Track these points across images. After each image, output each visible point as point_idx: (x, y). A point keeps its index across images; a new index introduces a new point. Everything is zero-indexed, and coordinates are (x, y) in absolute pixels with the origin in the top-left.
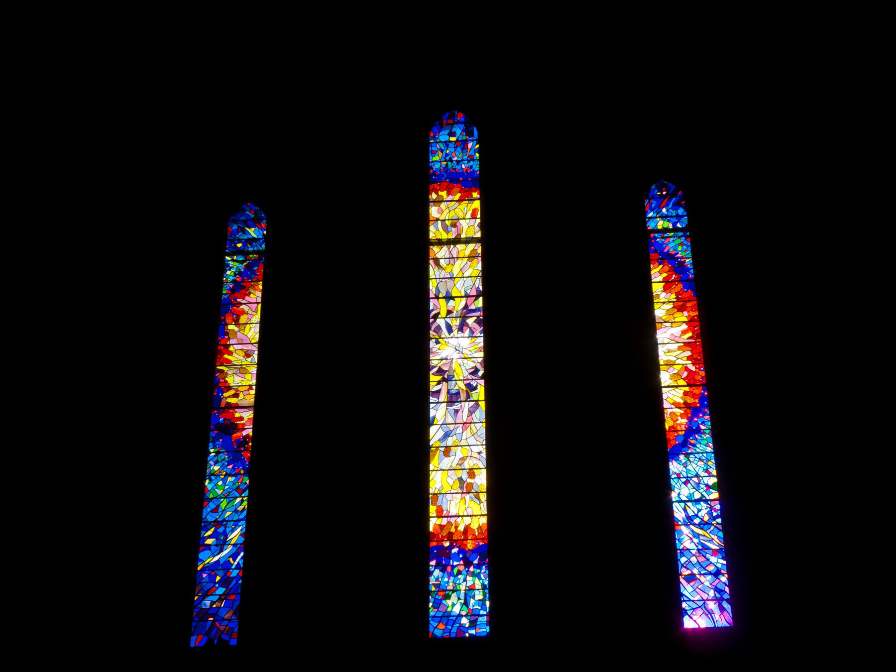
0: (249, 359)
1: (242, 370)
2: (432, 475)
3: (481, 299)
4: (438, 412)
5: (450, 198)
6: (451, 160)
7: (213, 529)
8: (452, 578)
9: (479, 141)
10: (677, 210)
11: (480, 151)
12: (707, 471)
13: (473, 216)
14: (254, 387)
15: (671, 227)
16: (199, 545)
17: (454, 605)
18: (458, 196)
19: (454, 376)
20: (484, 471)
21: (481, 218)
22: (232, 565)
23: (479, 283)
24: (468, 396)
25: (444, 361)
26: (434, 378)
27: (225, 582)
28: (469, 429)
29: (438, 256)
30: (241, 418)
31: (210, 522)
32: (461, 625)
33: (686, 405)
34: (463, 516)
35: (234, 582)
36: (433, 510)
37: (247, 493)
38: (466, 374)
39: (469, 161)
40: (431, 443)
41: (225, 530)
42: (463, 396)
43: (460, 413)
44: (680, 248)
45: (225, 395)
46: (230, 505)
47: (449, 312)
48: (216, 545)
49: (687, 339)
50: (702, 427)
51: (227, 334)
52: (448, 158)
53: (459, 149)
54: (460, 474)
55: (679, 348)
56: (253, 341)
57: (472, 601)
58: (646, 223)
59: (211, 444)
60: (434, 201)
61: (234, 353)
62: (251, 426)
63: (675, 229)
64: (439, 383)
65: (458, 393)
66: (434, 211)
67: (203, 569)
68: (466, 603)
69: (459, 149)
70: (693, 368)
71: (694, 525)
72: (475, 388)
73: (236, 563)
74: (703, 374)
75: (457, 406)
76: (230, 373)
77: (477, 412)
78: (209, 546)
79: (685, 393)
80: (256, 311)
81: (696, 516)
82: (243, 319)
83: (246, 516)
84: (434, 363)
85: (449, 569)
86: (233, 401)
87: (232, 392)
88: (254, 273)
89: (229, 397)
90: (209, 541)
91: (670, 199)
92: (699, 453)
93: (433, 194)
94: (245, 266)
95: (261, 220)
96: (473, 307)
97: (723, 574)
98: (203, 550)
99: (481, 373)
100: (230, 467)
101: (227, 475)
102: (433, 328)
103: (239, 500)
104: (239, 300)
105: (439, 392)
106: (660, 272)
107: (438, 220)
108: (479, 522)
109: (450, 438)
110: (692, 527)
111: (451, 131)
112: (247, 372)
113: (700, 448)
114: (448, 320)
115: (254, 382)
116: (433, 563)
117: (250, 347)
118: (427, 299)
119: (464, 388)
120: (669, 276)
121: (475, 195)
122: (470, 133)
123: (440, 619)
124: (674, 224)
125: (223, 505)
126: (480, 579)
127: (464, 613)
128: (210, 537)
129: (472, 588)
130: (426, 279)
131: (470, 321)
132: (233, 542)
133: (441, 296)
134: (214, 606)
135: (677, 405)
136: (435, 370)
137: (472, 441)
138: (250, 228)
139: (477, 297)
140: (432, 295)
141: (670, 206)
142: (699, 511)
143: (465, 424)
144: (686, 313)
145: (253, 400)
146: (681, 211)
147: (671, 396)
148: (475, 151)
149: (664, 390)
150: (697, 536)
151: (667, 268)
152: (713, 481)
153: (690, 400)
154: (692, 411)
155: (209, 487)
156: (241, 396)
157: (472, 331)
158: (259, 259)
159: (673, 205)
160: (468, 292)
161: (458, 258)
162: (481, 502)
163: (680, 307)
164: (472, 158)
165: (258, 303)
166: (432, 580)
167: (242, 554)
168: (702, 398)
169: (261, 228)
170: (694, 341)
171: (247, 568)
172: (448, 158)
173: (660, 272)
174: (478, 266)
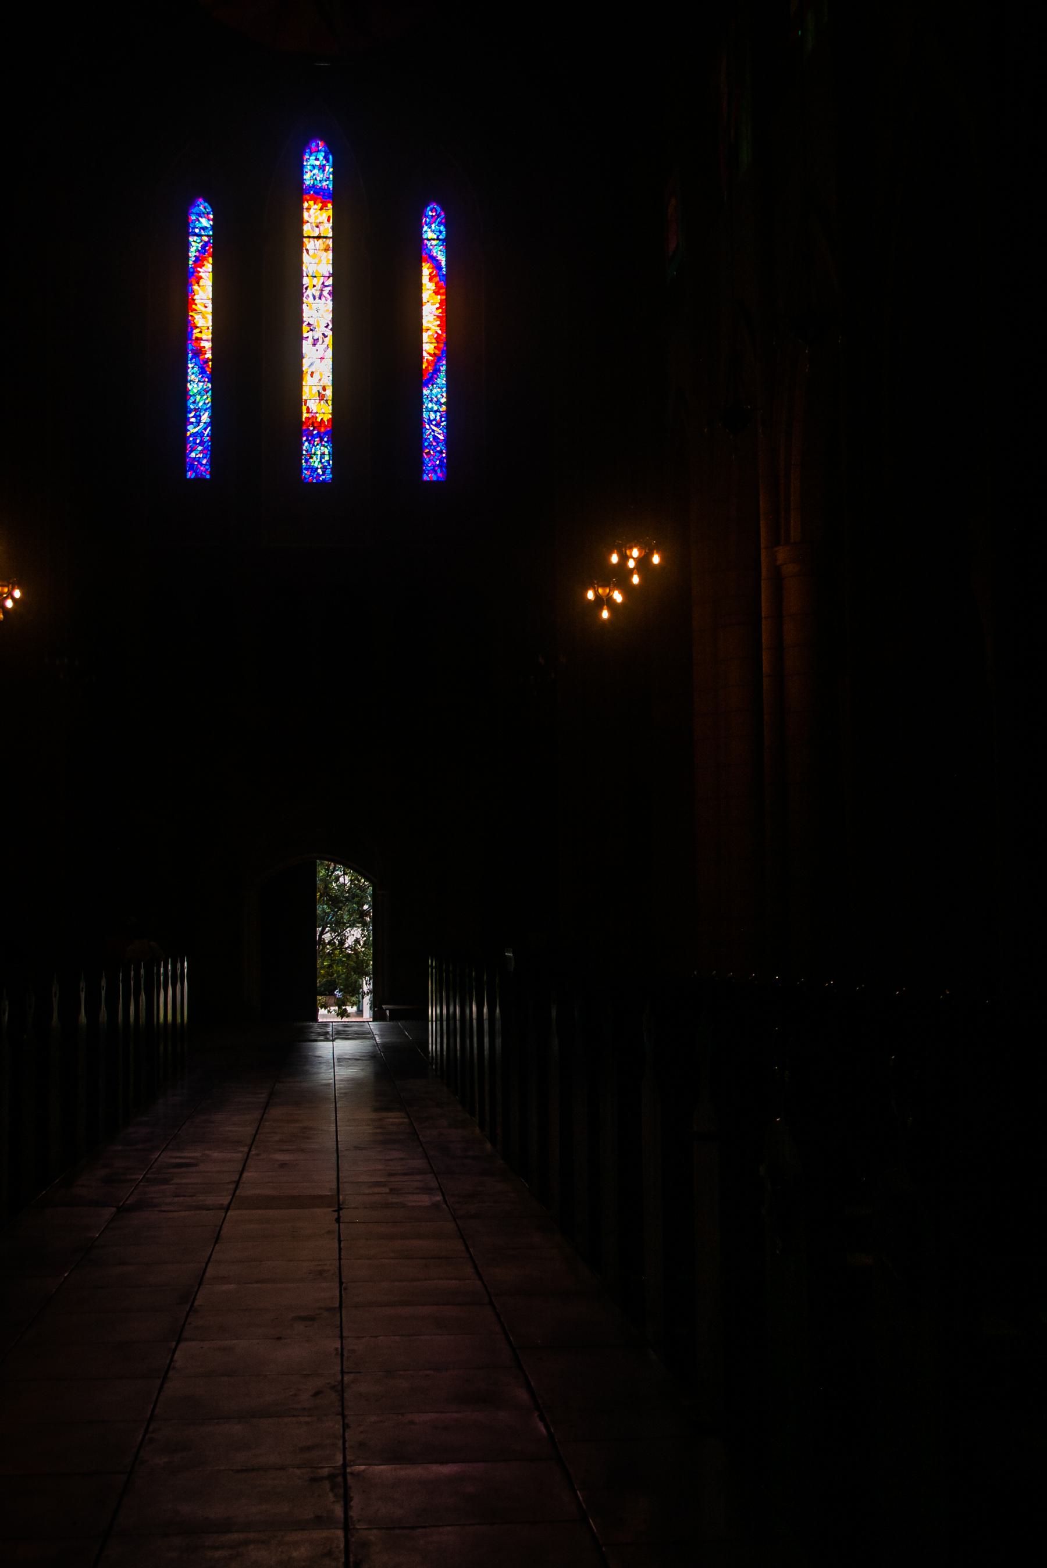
1: (204, 317)
3: (331, 278)
4: (307, 346)
5: (316, 207)
6: (316, 179)
8: (314, 447)
9: (334, 167)
10: (440, 226)
11: (333, 173)
12: (442, 395)
13: (328, 220)
14: (211, 328)
15: (435, 237)
16: (186, 422)
17: (315, 462)
18: (320, 205)
20: (331, 388)
21: (333, 223)
22: (204, 434)
23: (330, 269)
24: (323, 341)
26: (305, 328)
27: (202, 443)
29: (308, 247)
30: (204, 347)
31: (192, 409)
32: (318, 474)
33: (433, 355)
35: (207, 443)
36: (304, 408)
37: (210, 393)
39: (326, 181)
42: (321, 341)
44: (439, 253)
45: (195, 331)
48: (196, 422)
49: (440, 313)
50: (442, 369)
51: (193, 292)
53: (321, 171)
57: (323, 460)
58: (422, 234)
59: (189, 362)
60: (307, 209)
61: (198, 305)
62: (211, 352)
63: (438, 239)
65: (318, 339)
66: (306, 215)
67: (190, 436)
68: (321, 461)
69: (321, 171)
70: (440, 332)
71: (433, 425)
72: (327, 336)
74: (444, 335)
78: (192, 423)
79: (435, 347)
81: (435, 420)
82: (202, 282)
83: (210, 406)
84: (304, 319)
85: (312, 442)
86: (199, 335)
87: (198, 330)
88: (206, 251)
91: (437, 219)
92: (438, 384)
93: (306, 202)
94: (202, 246)
95: (208, 213)
96: (326, 284)
97: (444, 453)
98: (189, 425)
99: (330, 326)
101: (199, 381)
102: (305, 295)
103: (205, 397)
104: (199, 269)
105: (308, 337)
107: (308, 222)
110: (432, 426)
111: (316, 156)
113: (439, 381)
116: (304, 439)
119: (322, 336)
120: (433, 272)
121: (330, 206)
122: (327, 161)
123: (307, 469)
124: (438, 236)
125: (197, 400)
127: (319, 467)
128: (192, 417)
129: (323, 454)
131: (325, 293)
132: (204, 421)
134: (197, 456)
135: (429, 353)
139: (329, 277)
140: (305, 274)
141: (437, 223)
142: (436, 417)
144: (439, 297)
146: (442, 228)
149: (424, 345)
150: (433, 431)
151: (431, 266)
152: (443, 400)
153: (437, 352)
154: (437, 358)
155: (189, 386)
158: (209, 241)
159: (438, 224)
163: (436, 293)
164: (328, 178)
165: (209, 272)
166: (304, 448)
167: (209, 428)
169: (209, 219)
170: (441, 315)
171: (212, 436)
172: (314, 177)
174: (330, 255)
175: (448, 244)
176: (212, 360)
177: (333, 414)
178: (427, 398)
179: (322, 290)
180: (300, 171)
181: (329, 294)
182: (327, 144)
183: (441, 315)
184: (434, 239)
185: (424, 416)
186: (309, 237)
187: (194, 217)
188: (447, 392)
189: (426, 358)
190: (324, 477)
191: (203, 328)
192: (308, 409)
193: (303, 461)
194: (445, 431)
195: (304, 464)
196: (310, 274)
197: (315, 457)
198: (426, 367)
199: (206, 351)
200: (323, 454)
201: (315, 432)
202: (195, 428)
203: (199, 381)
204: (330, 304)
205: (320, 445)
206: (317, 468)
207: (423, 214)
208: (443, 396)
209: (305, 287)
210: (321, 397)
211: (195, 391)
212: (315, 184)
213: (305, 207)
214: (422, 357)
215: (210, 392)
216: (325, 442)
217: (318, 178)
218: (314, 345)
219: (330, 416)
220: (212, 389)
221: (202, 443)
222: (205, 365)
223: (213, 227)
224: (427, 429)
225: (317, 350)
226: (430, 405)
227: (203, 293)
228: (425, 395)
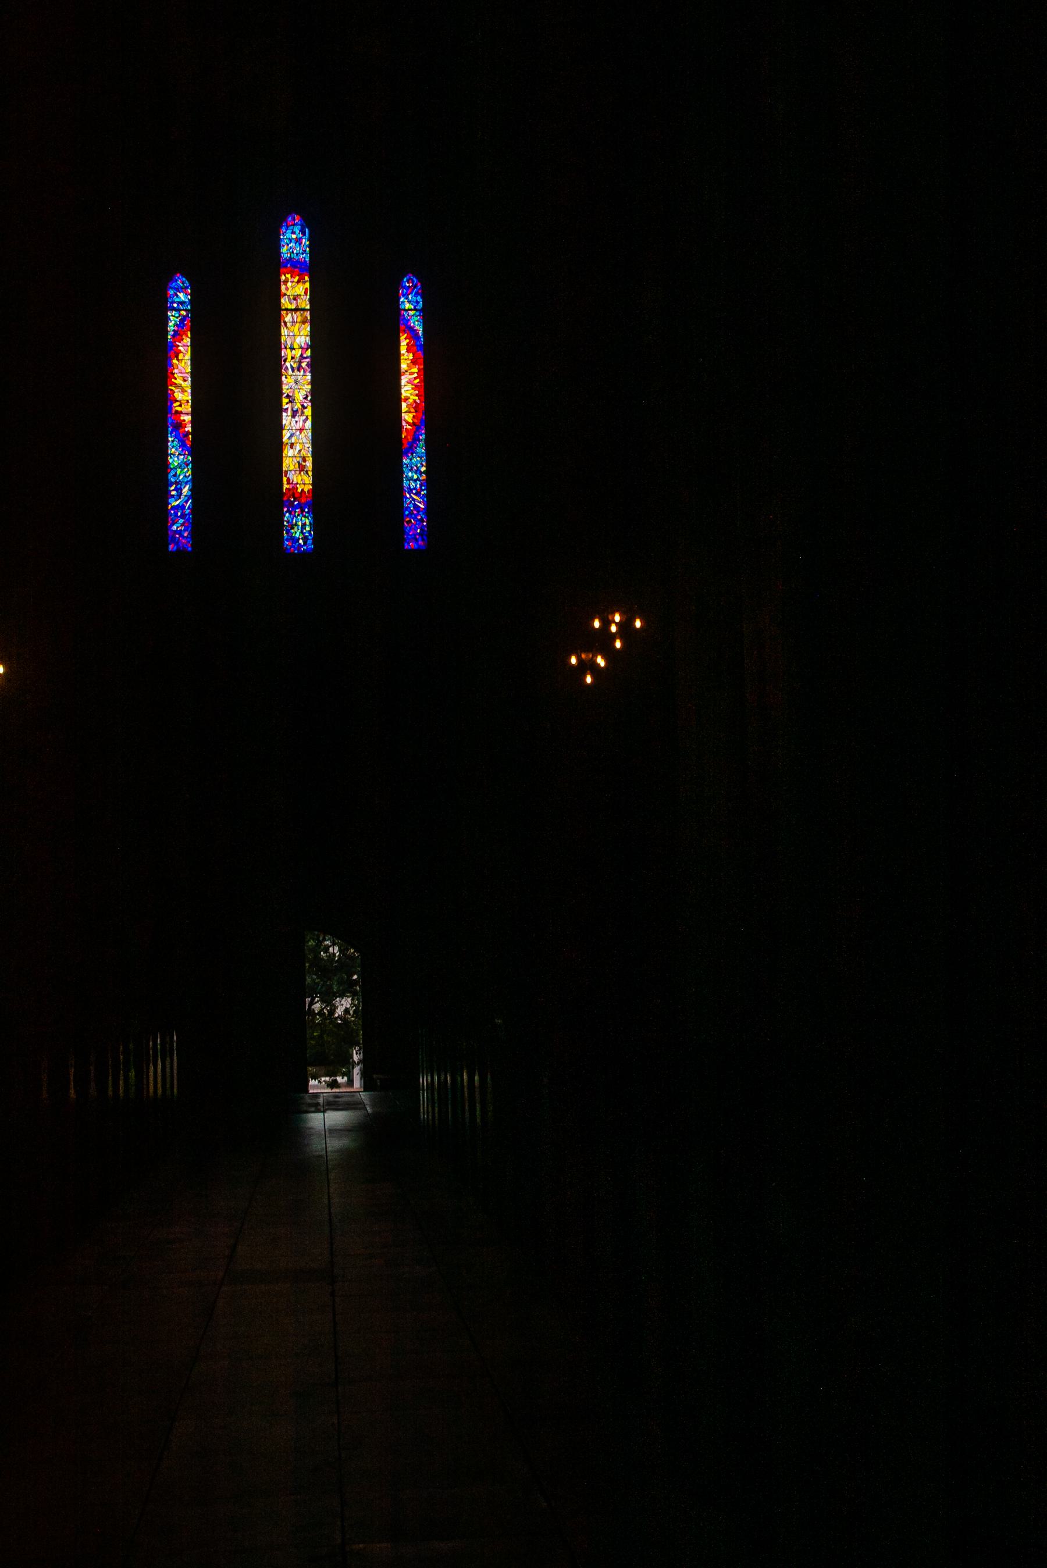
0: (186, 383)
1: (183, 391)
2: (284, 459)
3: (309, 350)
4: (286, 419)
7: (174, 486)
10: (417, 297)
11: (309, 246)
13: (306, 293)
14: (190, 401)
15: (412, 307)
16: (167, 495)
18: (297, 278)
19: (295, 400)
20: (311, 459)
23: (308, 339)
25: (289, 390)
26: (285, 401)
27: (183, 516)
28: (303, 433)
29: (287, 319)
30: (184, 421)
31: (173, 483)
32: (300, 544)
33: (413, 424)
34: (300, 484)
36: (285, 479)
37: (190, 466)
38: (301, 399)
39: (303, 254)
40: (284, 440)
41: (181, 488)
43: (298, 422)
44: (416, 323)
45: (175, 405)
46: (182, 472)
47: (293, 358)
48: (177, 495)
50: (421, 438)
51: (173, 366)
52: (291, 250)
53: (297, 244)
54: (298, 459)
55: (412, 389)
56: (187, 372)
57: (305, 531)
58: (399, 305)
59: (169, 435)
60: (284, 282)
62: (190, 425)
63: (415, 309)
64: (287, 403)
66: (283, 287)
68: (302, 532)
69: (297, 244)
70: (418, 401)
71: (414, 494)
72: (306, 408)
73: (187, 506)
75: (297, 419)
76: (176, 390)
77: (307, 422)
78: (173, 496)
79: (414, 417)
80: (187, 351)
82: (181, 356)
83: (190, 480)
86: (179, 409)
87: (178, 404)
89: (177, 406)
90: (173, 493)
95: (187, 288)
96: (305, 356)
97: (425, 522)
99: (309, 398)
100: (180, 450)
103: (186, 469)
104: (178, 343)
105: (287, 409)
106: (406, 339)
107: (285, 294)
108: (308, 488)
109: (293, 438)
110: (412, 495)
111: (293, 230)
112: (186, 391)
113: (418, 450)
114: (292, 363)
115: (190, 397)
116: (285, 509)
117: (186, 375)
118: (281, 349)
119: (300, 407)
121: (307, 278)
122: (304, 234)
123: (287, 540)
124: (415, 307)
125: (178, 472)
126: (308, 519)
127: (300, 537)
128: (173, 490)
130: (279, 335)
131: (304, 365)
132: (185, 494)
133: (288, 347)
135: (407, 422)
136: (285, 395)
137: (305, 440)
138: (180, 293)
139: (307, 349)
140: (283, 347)
141: (414, 294)
142: (416, 485)
143: (301, 430)
144: (417, 366)
145: (190, 409)
146: (419, 298)
147: (406, 418)
148: (307, 246)
149: (403, 415)
150: (414, 500)
152: (423, 469)
153: (416, 421)
156: (183, 405)
157: (305, 372)
158: (187, 315)
160: (303, 345)
161: (297, 322)
162: (309, 476)
163: (414, 362)
164: (305, 251)
166: (286, 519)
167: (190, 501)
168: (421, 420)
169: (187, 294)
170: (419, 384)
171: (193, 509)
172: (291, 250)
173: (406, 339)
174: (308, 328)
175: (426, 314)
176: (192, 433)
177: (312, 485)
178: (407, 467)
179: (300, 362)
180: (277, 245)
181: (307, 365)
182: (303, 218)
183: (419, 384)
184: (411, 310)
185: (404, 485)
186: (287, 310)
187: (172, 292)
188: (427, 461)
189: (405, 427)
190: (305, 548)
191: (182, 401)
192: (288, 480)
193: (285, 532)
194: (425, 499)
195: (285, 535)
196: (289, 346)
197: (296, 527)
198: (405, 437)
199: (186, 424)
200: (304, 525)
201: (296, 503)
202: (176, 501)
203: (179, 454)
204: (309, 377)
205: (301, 515)
206: (299, 539)
207: (399, 284)
208: (422, 465)
209: (283, 359)
210: (302, 468)
211: (176, 464)
212: (292, 256)
213: (282, 280)
214: (401, 427)
215: (191, 465)
216: (306, 512)
217: (295, 252)
218: (294, 416)
219: (311, 487)
220: (192, 462)
221: (183, 516)
222: (185, 439)
223: (191, 302)
224: (408, 498)
225: (296, 422)
226: (410, 474)
227: (183, 365)
228: (405, 464)
